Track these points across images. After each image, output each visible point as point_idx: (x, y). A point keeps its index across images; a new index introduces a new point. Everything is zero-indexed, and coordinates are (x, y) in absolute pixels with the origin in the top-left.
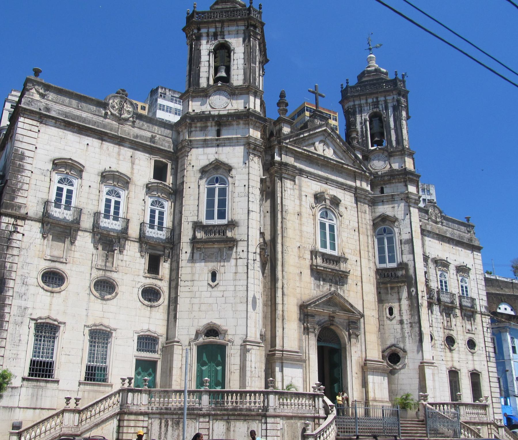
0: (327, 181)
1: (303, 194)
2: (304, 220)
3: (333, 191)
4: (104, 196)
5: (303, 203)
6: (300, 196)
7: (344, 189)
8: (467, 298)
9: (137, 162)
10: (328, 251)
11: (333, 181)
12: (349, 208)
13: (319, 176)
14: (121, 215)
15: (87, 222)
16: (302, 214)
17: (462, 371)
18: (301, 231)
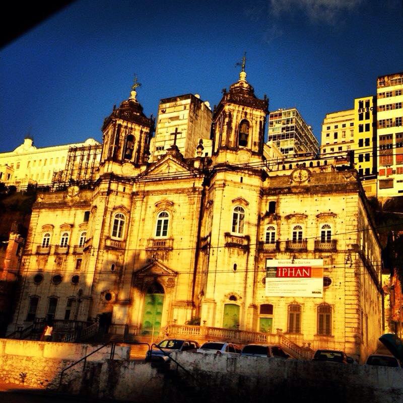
0: (166, 191)
1: (148, 206)
2: (146, 222)
3: (172, 197)
4: (62, 237)
5: (148, 212)
6: (146, 208)
7: (180, 193)
8: (329, 241)
9: (77, 216)
10: (161, 237)
11: (171, 190)
12: (181, 205)
13: (160, 191)
14: (68, 244)
15: (53, 251)
16: (146, 219)
17: (306, 305)
18: (143, 230)
